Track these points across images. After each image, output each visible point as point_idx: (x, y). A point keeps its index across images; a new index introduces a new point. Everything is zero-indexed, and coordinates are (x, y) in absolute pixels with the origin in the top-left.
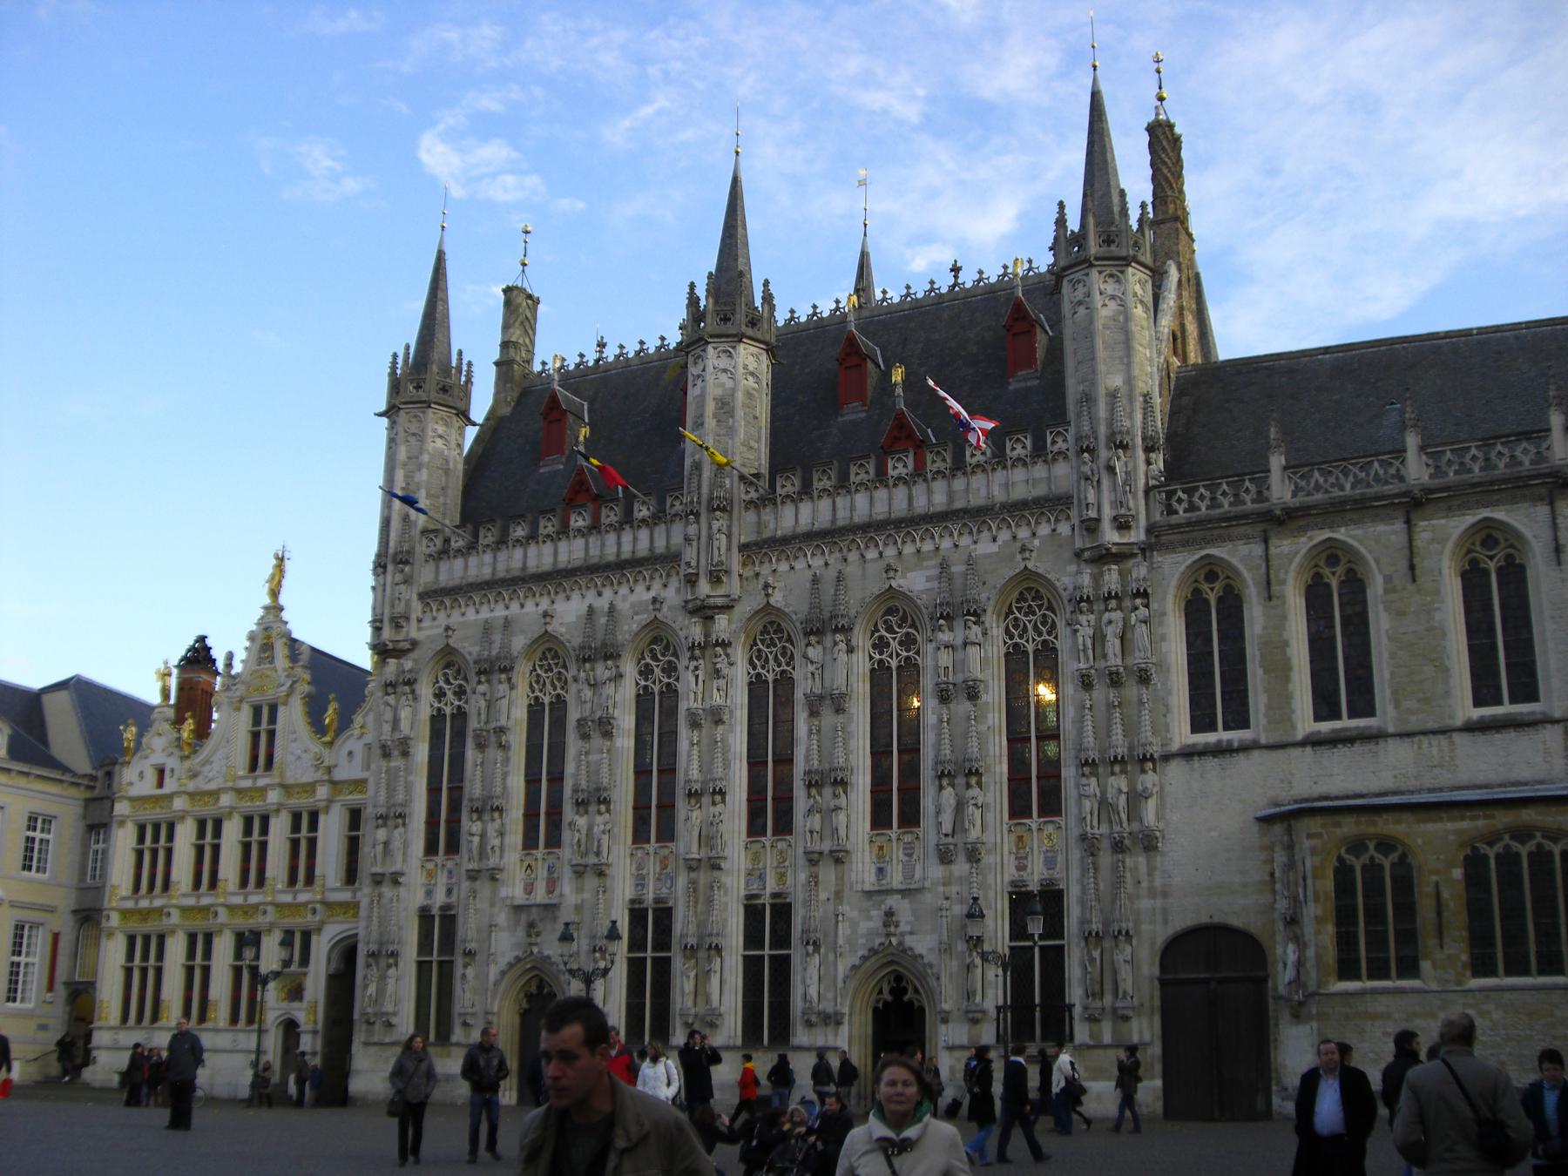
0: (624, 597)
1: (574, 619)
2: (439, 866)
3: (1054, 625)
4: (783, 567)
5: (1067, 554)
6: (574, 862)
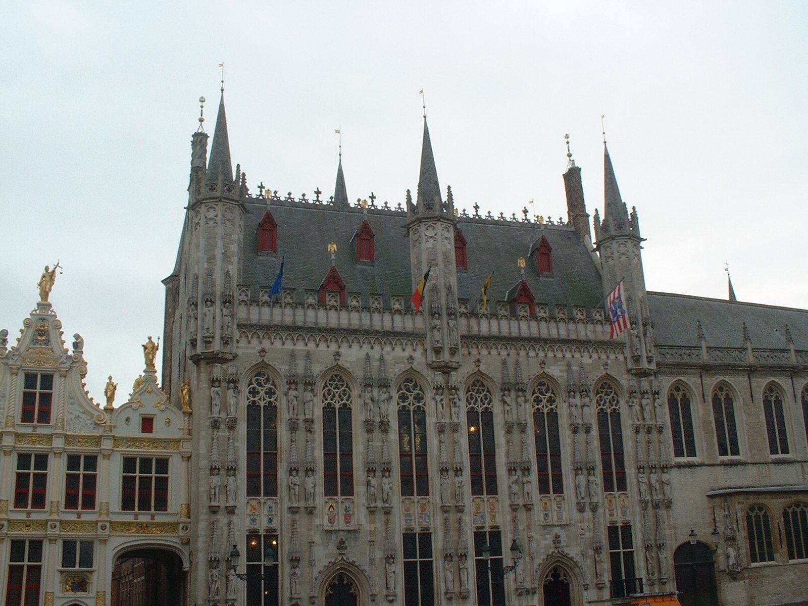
0: (388, 353)
1: (355, 359)
2: (262, 501)
3: (618, 402)
4: (484, 352)
5: (623, 370)
6: (372, 505)
